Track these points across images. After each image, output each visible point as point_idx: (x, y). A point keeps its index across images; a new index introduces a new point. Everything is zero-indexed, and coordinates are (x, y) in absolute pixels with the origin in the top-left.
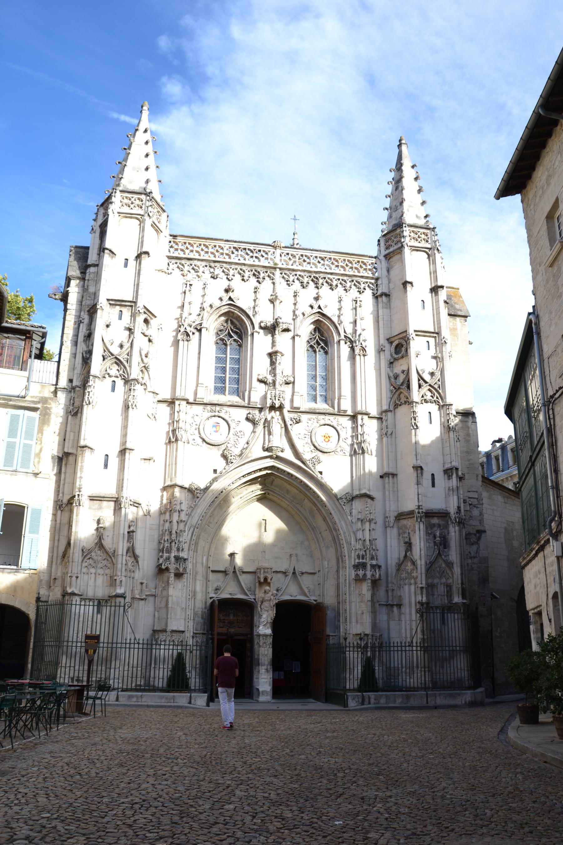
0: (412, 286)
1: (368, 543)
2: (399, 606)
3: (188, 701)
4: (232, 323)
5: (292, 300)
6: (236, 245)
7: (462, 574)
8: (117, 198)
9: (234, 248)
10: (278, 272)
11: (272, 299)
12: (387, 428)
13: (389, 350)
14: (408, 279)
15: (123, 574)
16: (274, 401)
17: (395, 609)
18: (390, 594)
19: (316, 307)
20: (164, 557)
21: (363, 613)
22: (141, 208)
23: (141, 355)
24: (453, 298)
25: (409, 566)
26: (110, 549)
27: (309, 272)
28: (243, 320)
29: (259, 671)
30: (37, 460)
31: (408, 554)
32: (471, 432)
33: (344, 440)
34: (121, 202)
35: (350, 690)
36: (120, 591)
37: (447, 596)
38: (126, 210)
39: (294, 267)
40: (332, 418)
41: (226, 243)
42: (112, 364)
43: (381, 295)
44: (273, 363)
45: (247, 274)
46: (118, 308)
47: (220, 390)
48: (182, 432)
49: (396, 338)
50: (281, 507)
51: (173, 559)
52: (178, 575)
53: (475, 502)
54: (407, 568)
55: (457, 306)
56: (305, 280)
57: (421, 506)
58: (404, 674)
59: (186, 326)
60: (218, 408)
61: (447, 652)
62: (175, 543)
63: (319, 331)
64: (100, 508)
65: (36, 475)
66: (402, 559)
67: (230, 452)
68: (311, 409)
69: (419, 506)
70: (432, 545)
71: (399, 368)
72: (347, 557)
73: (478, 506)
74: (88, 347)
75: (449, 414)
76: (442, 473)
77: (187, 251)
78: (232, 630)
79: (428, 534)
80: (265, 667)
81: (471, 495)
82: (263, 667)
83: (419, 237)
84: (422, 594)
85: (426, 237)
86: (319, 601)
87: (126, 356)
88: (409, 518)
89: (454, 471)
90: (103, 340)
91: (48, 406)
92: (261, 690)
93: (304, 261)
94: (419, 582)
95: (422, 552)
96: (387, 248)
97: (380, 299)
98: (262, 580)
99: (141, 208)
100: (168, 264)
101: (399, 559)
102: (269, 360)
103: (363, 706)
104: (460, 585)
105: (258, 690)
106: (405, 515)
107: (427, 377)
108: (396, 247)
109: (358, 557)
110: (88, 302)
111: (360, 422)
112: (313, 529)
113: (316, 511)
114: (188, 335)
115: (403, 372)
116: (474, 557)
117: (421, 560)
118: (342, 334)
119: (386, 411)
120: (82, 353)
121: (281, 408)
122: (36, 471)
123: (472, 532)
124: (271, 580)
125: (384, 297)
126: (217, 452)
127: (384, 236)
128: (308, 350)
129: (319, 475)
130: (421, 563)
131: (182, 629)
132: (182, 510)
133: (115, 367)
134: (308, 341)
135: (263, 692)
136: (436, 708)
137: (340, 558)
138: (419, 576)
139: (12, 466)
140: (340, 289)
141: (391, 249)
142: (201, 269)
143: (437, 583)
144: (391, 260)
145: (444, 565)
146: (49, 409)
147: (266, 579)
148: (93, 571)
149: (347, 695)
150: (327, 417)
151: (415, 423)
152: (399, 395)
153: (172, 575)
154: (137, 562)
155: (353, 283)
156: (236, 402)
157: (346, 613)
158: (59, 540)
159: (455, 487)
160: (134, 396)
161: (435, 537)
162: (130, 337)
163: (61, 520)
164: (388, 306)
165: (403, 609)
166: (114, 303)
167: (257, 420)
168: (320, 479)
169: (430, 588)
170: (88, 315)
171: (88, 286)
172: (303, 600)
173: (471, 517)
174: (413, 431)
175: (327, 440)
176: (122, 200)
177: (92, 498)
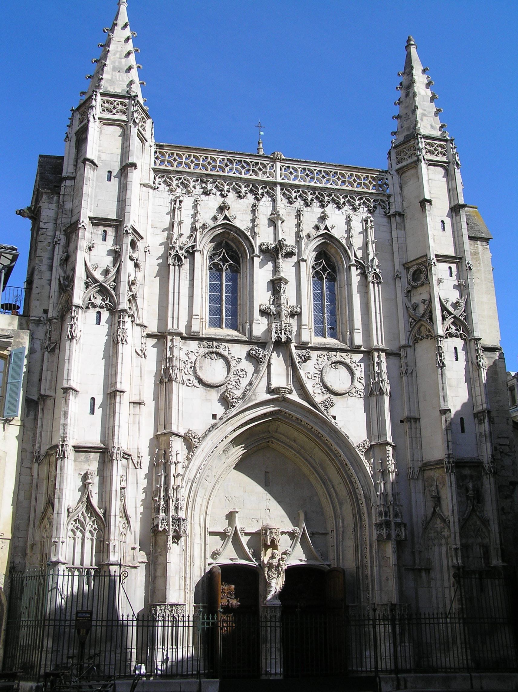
0: (431, 204)
1: (390, 498)
2: (428, 570)
5: (295, 221)
9: (228, 160)
10: (279, 188)
11: (273, 218)
12: (407, 366)
13: (406, 277)
14: (427, 197)
16: (280, 335)
17: (423, 574)
18: (417, 556)
19: (322, 227)
25: (439, 524)
27: (314, 188)
28: (240, 242)
32: (498, 369)
33: (359, 380)
39: (297, 182)
40: (344, 354)
43: (394, 215)
45: (243, 190)
46: (102, 228)
48: (177, 371)
53: (507, 449)
54: (436, 526)
56: (310, 197)
59: (177, 248)
60: (215, 344)
66: (429, 515)
69: (449, 455)
71: (418, 297)
72: (366, 514)
73: (510, 454)
74: (65, 272)
79: (459, 486)
81: (502, 441)
83: (435, 150)
84: (457, 556)
86: (333, 566)
87: (113, 283)
95: (455, 508)
97: (393, 219)
100: (155, 178)
101: (426, 516)
104: (499, 546)
108: (410, 161)
109: (380, 514)
110: (65, 221)
115: (424, 301)
117: (454, 517)
118: (353, 258)
119: (405, 347)
120: (59, 279)
125: (397, 216)
126: (215, 395)
127: (395, 147)
129: (333, 421)
130: (454, 521)
132: (178, 462)
134: (313, 267)
137: (358, 516)
138: (453, 535)
140: (347, 207)
141: (404, 163)
142: (192, 184)
144: (404, 175)
145: (478, 523)
149: (379, 678)
150: (339, 354)
151: (441, 360)
152: (420, 328)
153: (171, 538)
154: (129, 523)
157: (367, 579)
158: (36, 499)
159: (487, 433)
161: (467, 490)
164: (402, 226)
165: (433, 575)
166: (96, 222)
167: (260, 356)
169: (465, 547)
170: (64, 235)
171: (63, 202)
172: (314, 565)
173: (503, 466)
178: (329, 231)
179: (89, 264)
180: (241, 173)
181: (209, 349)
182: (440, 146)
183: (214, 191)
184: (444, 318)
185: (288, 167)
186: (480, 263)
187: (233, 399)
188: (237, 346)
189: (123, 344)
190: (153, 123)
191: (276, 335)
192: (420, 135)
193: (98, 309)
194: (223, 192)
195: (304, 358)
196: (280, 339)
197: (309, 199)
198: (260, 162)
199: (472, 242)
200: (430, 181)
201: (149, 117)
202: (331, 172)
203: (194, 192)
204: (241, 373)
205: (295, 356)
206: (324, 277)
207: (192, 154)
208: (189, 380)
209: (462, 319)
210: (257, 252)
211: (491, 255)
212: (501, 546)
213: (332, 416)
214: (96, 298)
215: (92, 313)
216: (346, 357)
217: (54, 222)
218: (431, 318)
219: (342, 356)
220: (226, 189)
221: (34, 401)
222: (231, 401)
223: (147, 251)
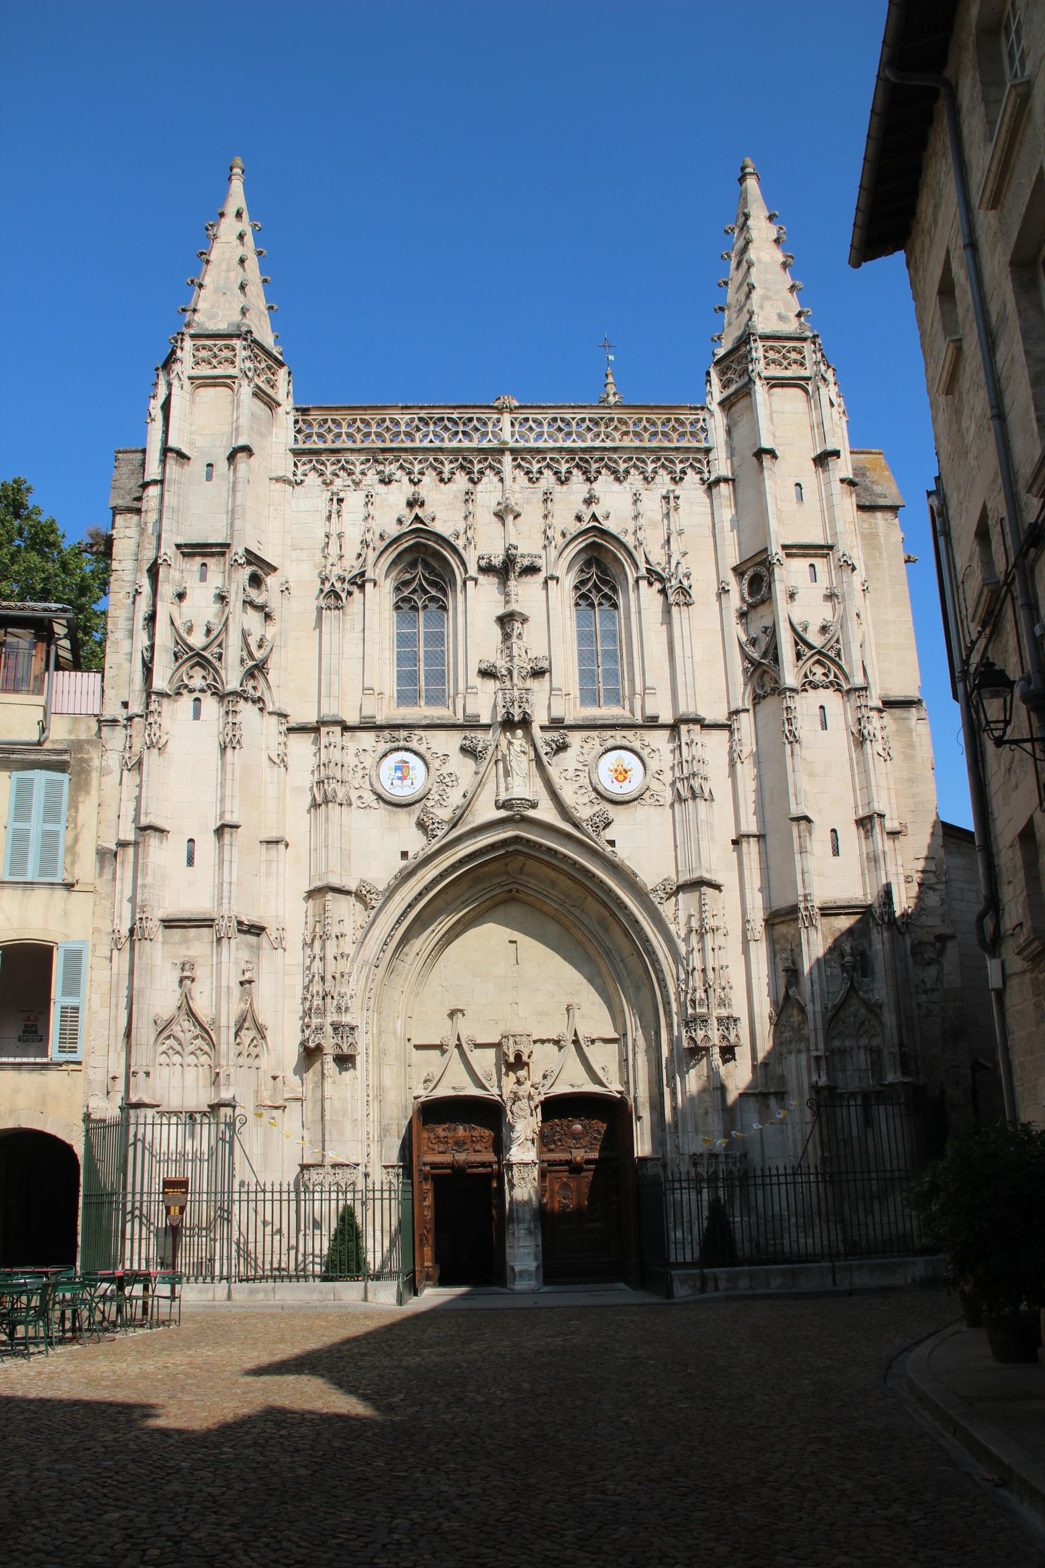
3: (362, 1295)
4: (427, 565)
6: (423, 414)
7: (899, 1026)
8: (187, 351)
9: (421, 419)
10: (507, 458)
11: (500, 511)
14: (766, 444)
15: (231, 1063)
17: (772, 1102)
20: (313, 1027)
21: (706, 1113)
22: (233, 363)
23: (247, 645)
24: (868, 474)
26: (206, 1017)
27: (571, 451)
29: (514, 1233)
30: (69, 859)
31: (790, 993)
32: (915, 739)
33: (657, 776)
34: (194, 356)
35: (677, 1265)
36: (226, 1095)
37: (872, 1070)
38: (205, 370)
39: (540, 444)
41: (404, 411)
42: (192, 667)
44: (507, 636)
45: (447, 468)
46: (199, 560)
47: (406, 698)
49: (749, 564)
50: (546, 914)
51: (329, 1030)
52: (345, 1061)
55: (877, 489)
56: (564, 467)
57: (810, 895)
58: (793, 1229)
60: (404, 734)
61: (874, 1182)
62: (332, 998)
63: (600, 564)
64: (186, 941)
65: (69, 886)
68: (587, 719)
70: (837, 971)
73: (938, 887)
75: (860, 707)
76: (854, 826)
77: (330, 437)
78: (461, 1157)
80: (525, 1225)
82: (521, 1226)
84: (818, 1070)
85: (798, 357)
88: (790, 920)
89: (877, 820)
90: (172, 623)
91: (85, 756)
92: (517, 1269)
93: (560, 429)
94: (812, 1047)
95: (816, 987)
96: (724, 387)
98: (512, 1059)
99: (233, 363)
100: (296, 465)
102: (499, 632)
103: (703, 1296)
104: (897, 1048)
105: (512, 1268)
106: (782, 915)
107: (815, 639)
108: (741, 383)
111: (684, 738)
112: (608, 953)
113: (610, 919)
114: (338, 597)
116: (933, 990)
118: (643, 566)
121: (525, 723)
122: (70, 880)
123: (925, 939)
124: (529, 1057)
125: (722, 485)
128: (577, 604)
129: (609, 848)
131: (353, 1160)
133: (198, 672)
135: (521, 1272)
136: (850, 1293)
139: (25, 875)
140: (635, 477)
141: (733, 388)
142: (359, 468)
143: (852, 1049)
144: (733, 410)
145: (863, 1011)
146: (87, 761)
147: (518, 1056)
148: (177, 1059)
149: (671, 1275)
150: (618, 734)
151: (790, 731)
155: (659, 464)
156: (439, 719)
160: (234, 724)
162: (223, 613)
163: (119, 968)
167: (479, 749)
168: (609, 855)
172: (595, 1093)
174: (788, 747)
175: (621, 778)
176: (197, 353)
177: (169, 924)
179: (178, 623)
180: (442, 440)
182: (794, 349)
183: (399, 474)
184: (799, 656)
185: (526, 420)
186: (880, 553)
188: (441, 735)
189: (234, 748)
190: (290, 373)
191: (504, 710)
192: (754, 335)
193: (197, 695)
197: (563, 471)
198: (475, 416)
199: (865, 516)
200: (775, 415)
201: (281, 364)
202: (602, 419)
203: (364, 482)
204: (447, 779)
205: (539, 743)
207: (358, 417)
208: (360, 797)
209: (833, 655)
210: (473, 571)
211: (902, 535)
212: (900, 1049)
213: (607, 841)
214: (191, 677)
215: (186, 702)
216: (632, 738)
217: (134, 557)
218: (776, 659)
220: (416, 470)
221: (111, 850)
222: (431, 827)
223: (286, 590)
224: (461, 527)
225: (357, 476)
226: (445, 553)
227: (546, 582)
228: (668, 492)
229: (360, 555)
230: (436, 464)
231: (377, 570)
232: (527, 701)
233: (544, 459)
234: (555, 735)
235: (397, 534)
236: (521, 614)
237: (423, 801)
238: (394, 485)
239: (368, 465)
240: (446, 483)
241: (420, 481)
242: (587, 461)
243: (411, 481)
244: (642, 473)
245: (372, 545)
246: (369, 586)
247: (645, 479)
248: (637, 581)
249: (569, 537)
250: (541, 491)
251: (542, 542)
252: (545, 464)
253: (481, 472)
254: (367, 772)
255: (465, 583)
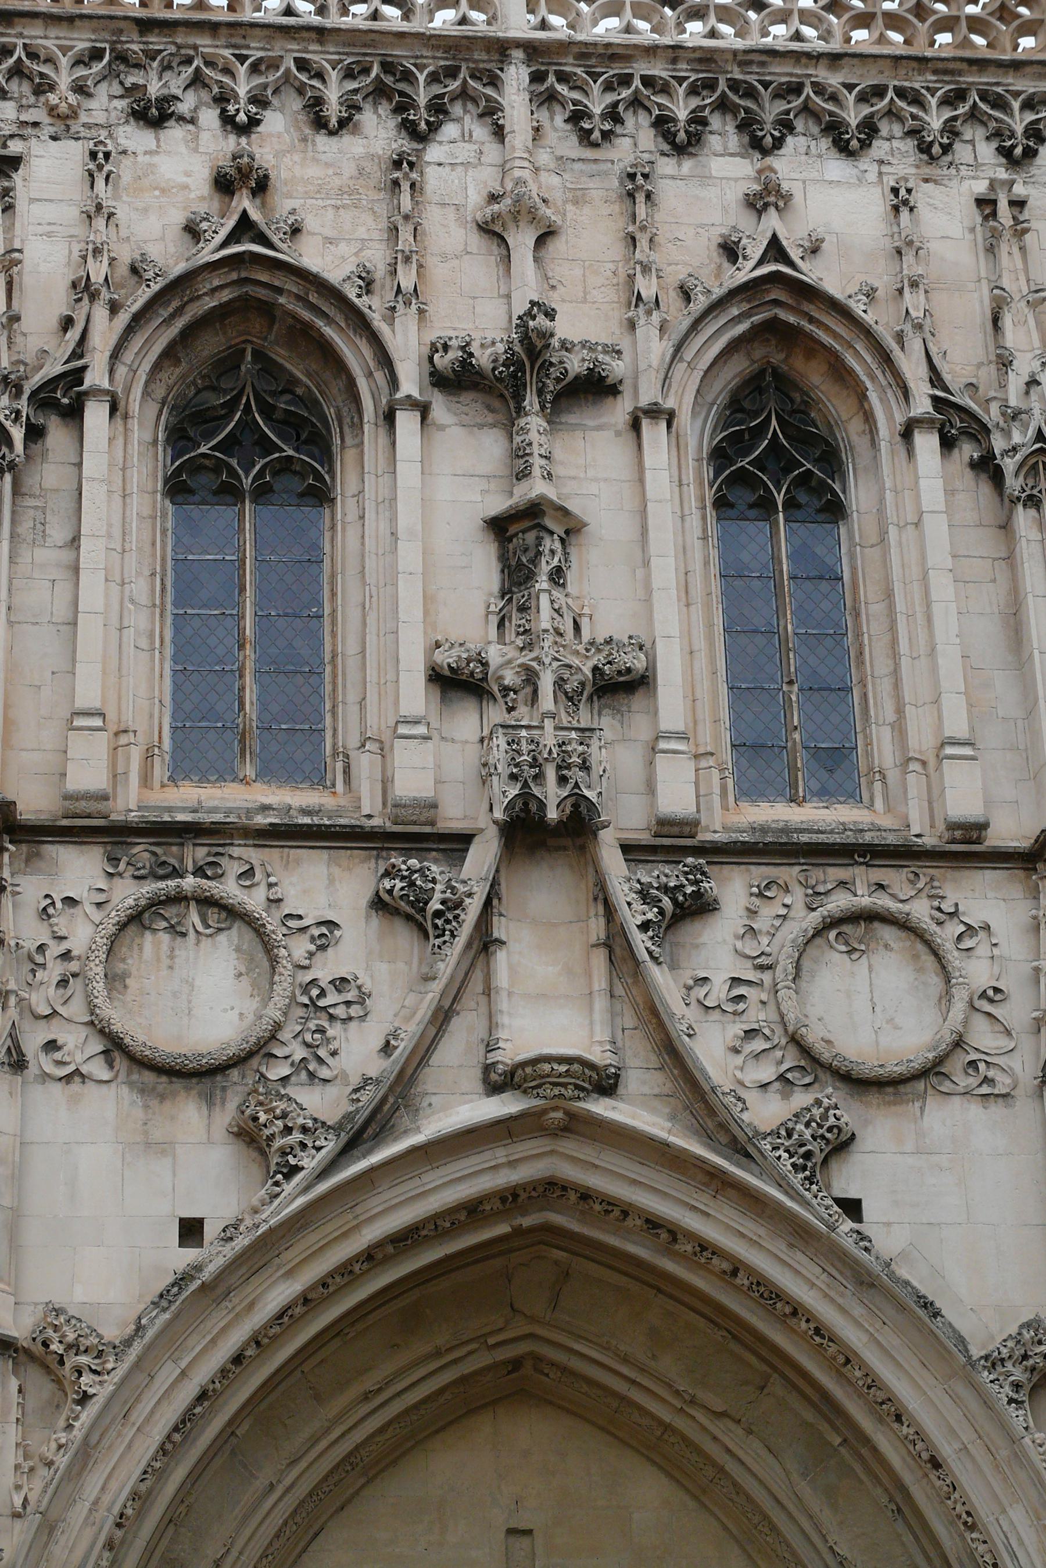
11: (496, 218)
16: (536, 791)
40: (896, 878)
60: (197, 853)
67: (280, 1106)
68: (764, 829)
129: (847, 1225)
150: (862, 876)
155: (963, 109)
156: (306, 812)
167: (435, 905)
168: (849, 1243)
178: (791, 264)
181: (161, 884)
187: (288, 1130)
191: (513, 791)
194: (231, 108)
195: (674, 900)
196: (533, 807)
197: (682, 114)
203: (84, 118)
205: (622, 892)
206: (780, 500)
208: (51, 1046)
210: (410, 385)
213: (839, 1202)
219: (881, 886)
222: (278, 1143)
224: (377, 257)
225: (63, 95)
226: (328, 331)
227: (635, 426)
228: (992, 187)
229: (67, 323)
230: (303, 77)
231: (122, 371)
232: (585, 767)
233: (625, 80)
234: (671, 874)
235: (179, 268)
236: (565, 512)
237: (254, 1062)
238: (175, 133)
239: (97, 67)
240: (332, 133)
241: (254, 122)
242: (750, 93)
243: (228, 121)
244: (912, 133)
245: (105, 295)
246: (95, 414)
247: (924, 148)
248: (907, 434)
249: (701, 302)
250: (617, 168)
251: (618, 314)
252: (626, 93)
253: (439, 108)
254: (74, 966)
255: (389, 418)
